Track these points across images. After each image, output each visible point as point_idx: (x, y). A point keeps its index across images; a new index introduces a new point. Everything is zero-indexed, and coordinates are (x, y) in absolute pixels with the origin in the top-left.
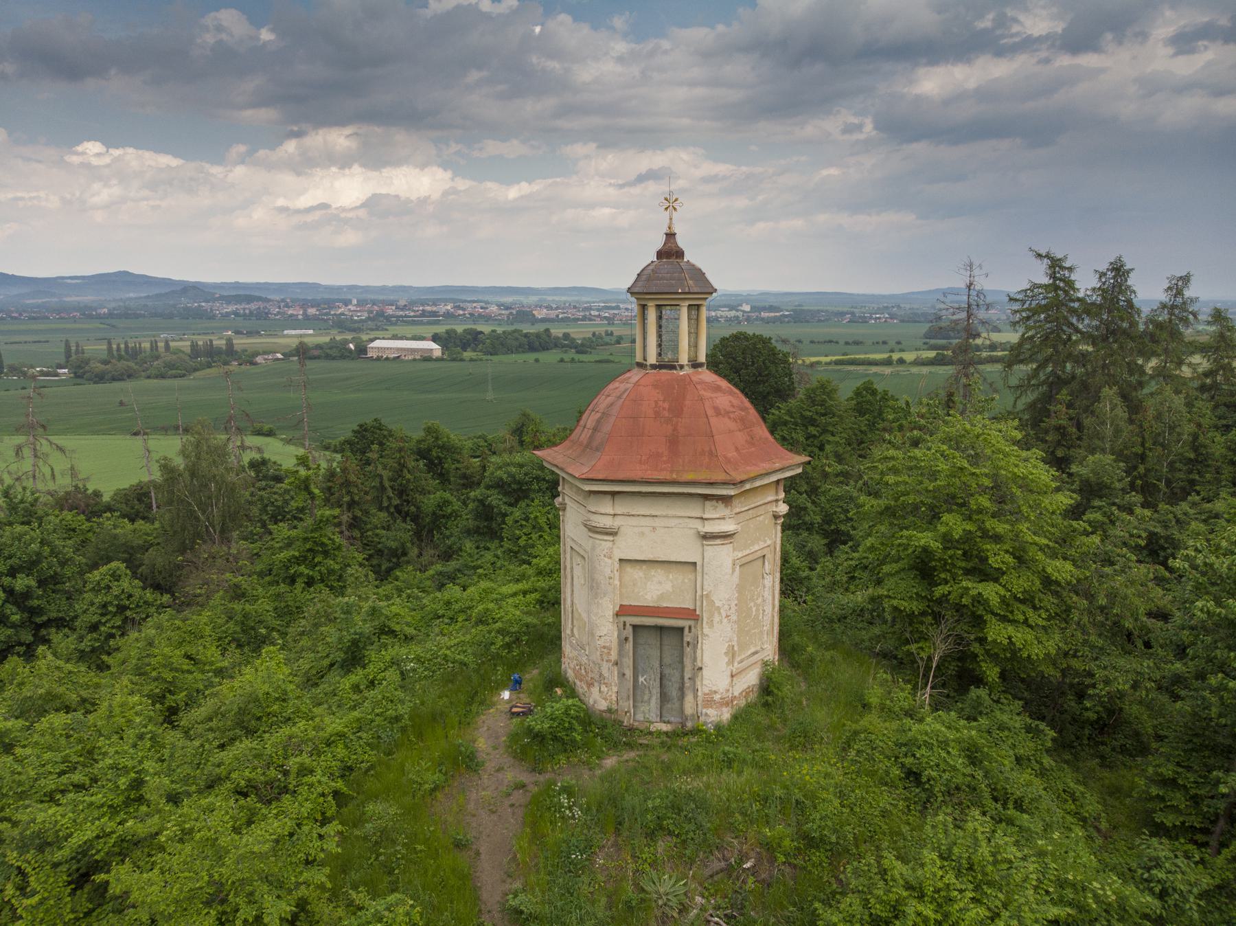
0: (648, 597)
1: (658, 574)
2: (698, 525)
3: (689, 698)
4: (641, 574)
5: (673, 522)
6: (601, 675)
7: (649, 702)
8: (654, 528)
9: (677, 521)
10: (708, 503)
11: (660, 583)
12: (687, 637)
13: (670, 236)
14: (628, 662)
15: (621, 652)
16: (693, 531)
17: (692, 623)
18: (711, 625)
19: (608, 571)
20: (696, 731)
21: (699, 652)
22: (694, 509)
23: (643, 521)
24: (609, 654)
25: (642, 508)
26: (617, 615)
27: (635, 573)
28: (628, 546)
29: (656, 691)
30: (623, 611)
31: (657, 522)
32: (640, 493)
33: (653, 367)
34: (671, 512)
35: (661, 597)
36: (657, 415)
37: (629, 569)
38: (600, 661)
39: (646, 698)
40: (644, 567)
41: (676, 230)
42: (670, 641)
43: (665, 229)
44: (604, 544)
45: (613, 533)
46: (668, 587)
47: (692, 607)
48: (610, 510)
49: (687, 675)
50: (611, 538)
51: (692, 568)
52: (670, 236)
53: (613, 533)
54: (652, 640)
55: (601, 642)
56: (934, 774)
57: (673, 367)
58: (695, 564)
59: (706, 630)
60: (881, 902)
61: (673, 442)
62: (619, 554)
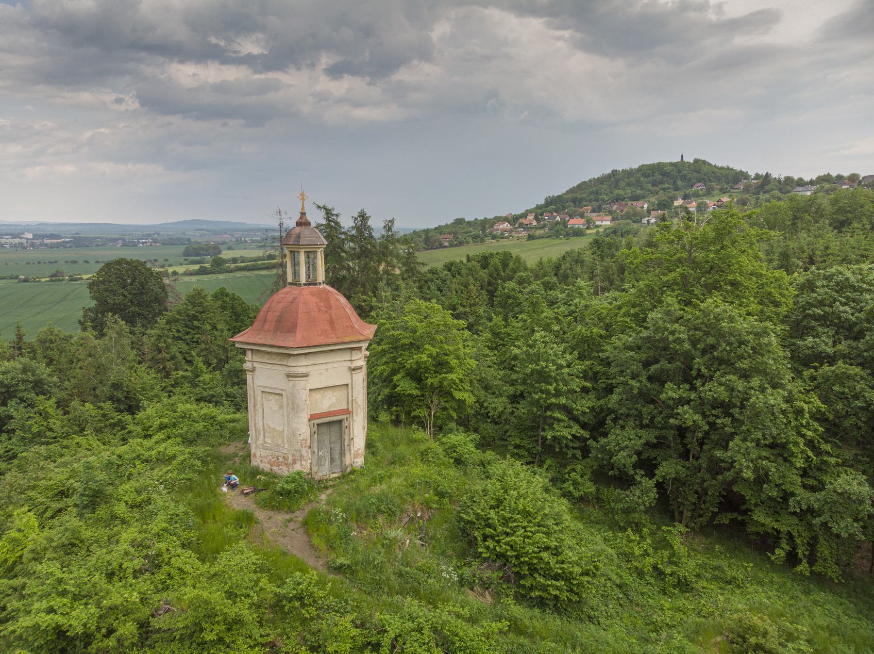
0: (324, 407)
1: (329, 394)
2: (349, 364)
3: (348, 456)
4: (320, 396)
5: (336, 365)
6: (301, 456)
7: (324, 465)
8: (327, 369)
9: (338, 364)
10: (353, 352)
11: (330, 399)
12: (345, 424)
13: (303, 214)
14: (315, 444)
15: (312, 442)
16: (347, 368)
17: (347, 416)
18: (357, 415)
19: (304, 397)
20: (353, 472)
21: (351, 430)
22: (347, 356)
23: (322, 367)
24: (306, 443)
25: (321, 359)
26: (309, 420)
27: (317, 396)
28: (314, 382)
29: (328, 458)
30: (312, 417)
31: (329, 366)
32: (324, 352)
33: (305, 284)
34: (336, 360)
35: (330, 406)
36: (319, 310)
37: (314, 394)
38: (300, 448)
39: (323, 463)
40: (321, 392)
41: (306, 211)
42: (335, 428)
43: (300, 210)
44: (301, 383)
45: (306, 375)
46: (334, 400)
47: (346, 408)
48: (304, 363)
49: (346, 443)
50: (305, 379)
51: (345, 387)
52: (303, 214)
53: (306, 375)
54: (324, 430)
55: (301, 438)
56: (467, 456)
57: (316, 284)
58: (348, 385)
59: (355, 418)
60: (493, 499)
61: (331, 323)
62: (309, 387)
